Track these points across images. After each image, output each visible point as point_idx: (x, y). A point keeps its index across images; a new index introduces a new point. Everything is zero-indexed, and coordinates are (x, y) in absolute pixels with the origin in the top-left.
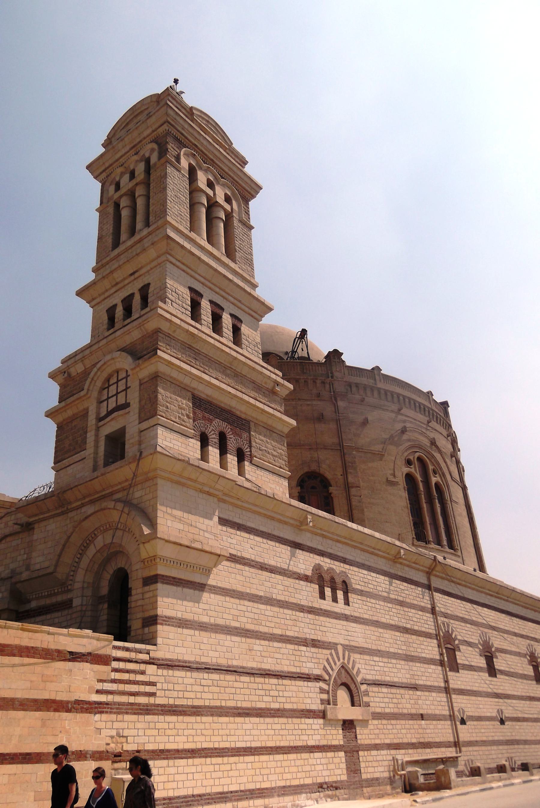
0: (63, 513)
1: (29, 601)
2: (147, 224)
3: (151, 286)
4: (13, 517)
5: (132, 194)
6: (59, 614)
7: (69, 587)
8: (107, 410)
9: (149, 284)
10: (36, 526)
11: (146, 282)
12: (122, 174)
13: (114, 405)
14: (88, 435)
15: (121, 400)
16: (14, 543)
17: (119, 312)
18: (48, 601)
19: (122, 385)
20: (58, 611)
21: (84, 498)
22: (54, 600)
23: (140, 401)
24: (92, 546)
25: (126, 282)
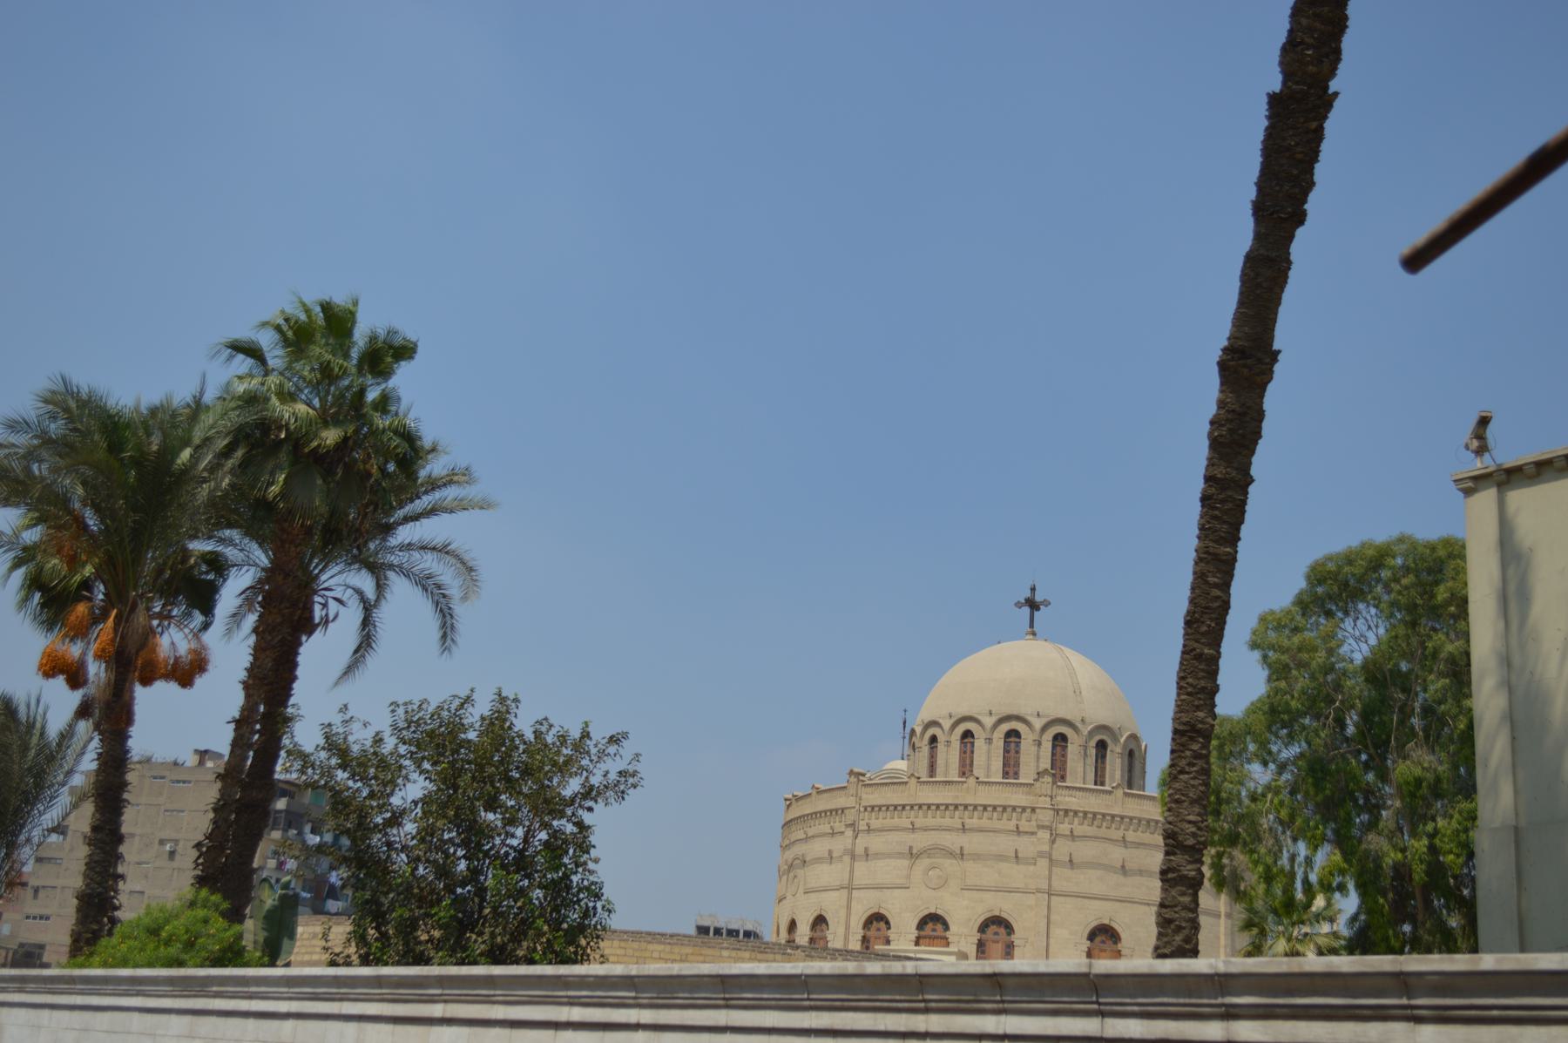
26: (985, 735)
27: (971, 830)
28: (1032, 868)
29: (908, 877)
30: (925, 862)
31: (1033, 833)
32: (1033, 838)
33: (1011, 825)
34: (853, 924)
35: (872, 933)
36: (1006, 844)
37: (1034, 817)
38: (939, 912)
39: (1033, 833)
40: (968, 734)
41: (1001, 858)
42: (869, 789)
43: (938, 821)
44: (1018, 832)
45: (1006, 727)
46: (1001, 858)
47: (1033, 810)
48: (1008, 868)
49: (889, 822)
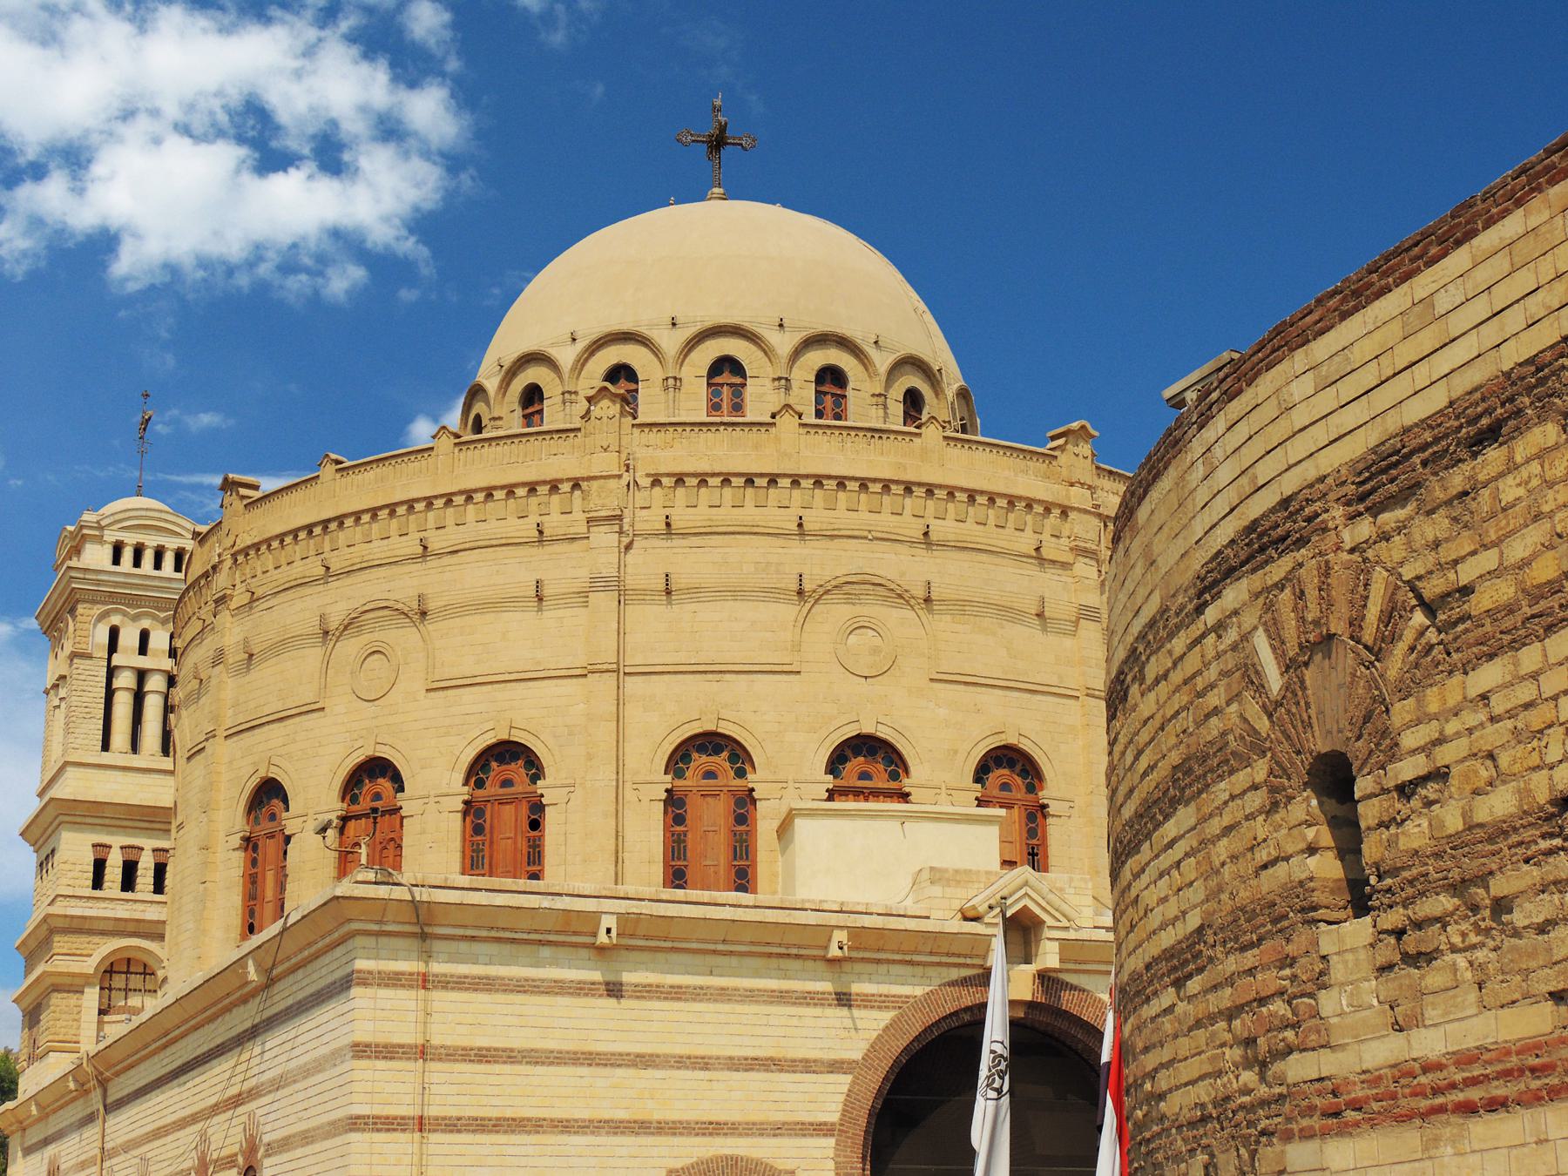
5: (142, 675)
26: (771, 371)
27: (943, 545)
28: (1068, 642)
29: (797, 647)
30: (835, 613)
31: (1065, 566)
32: (1065, 577)
33: (1026, 543)
34: (631, 762)
35: (691, 780)
36: (1020, 584)
37: (1066, 529)
38: (884, 733)
39: (1065, 566)
40: (726, 366)
41: (1008, 613)
42: (653, 437)
43: (863, 519)
44: (1038, 557)
45: (818, 358)
46: (1008, 613)
47: (1064, 513)
48: (1026, 635)
49: (726, 515)
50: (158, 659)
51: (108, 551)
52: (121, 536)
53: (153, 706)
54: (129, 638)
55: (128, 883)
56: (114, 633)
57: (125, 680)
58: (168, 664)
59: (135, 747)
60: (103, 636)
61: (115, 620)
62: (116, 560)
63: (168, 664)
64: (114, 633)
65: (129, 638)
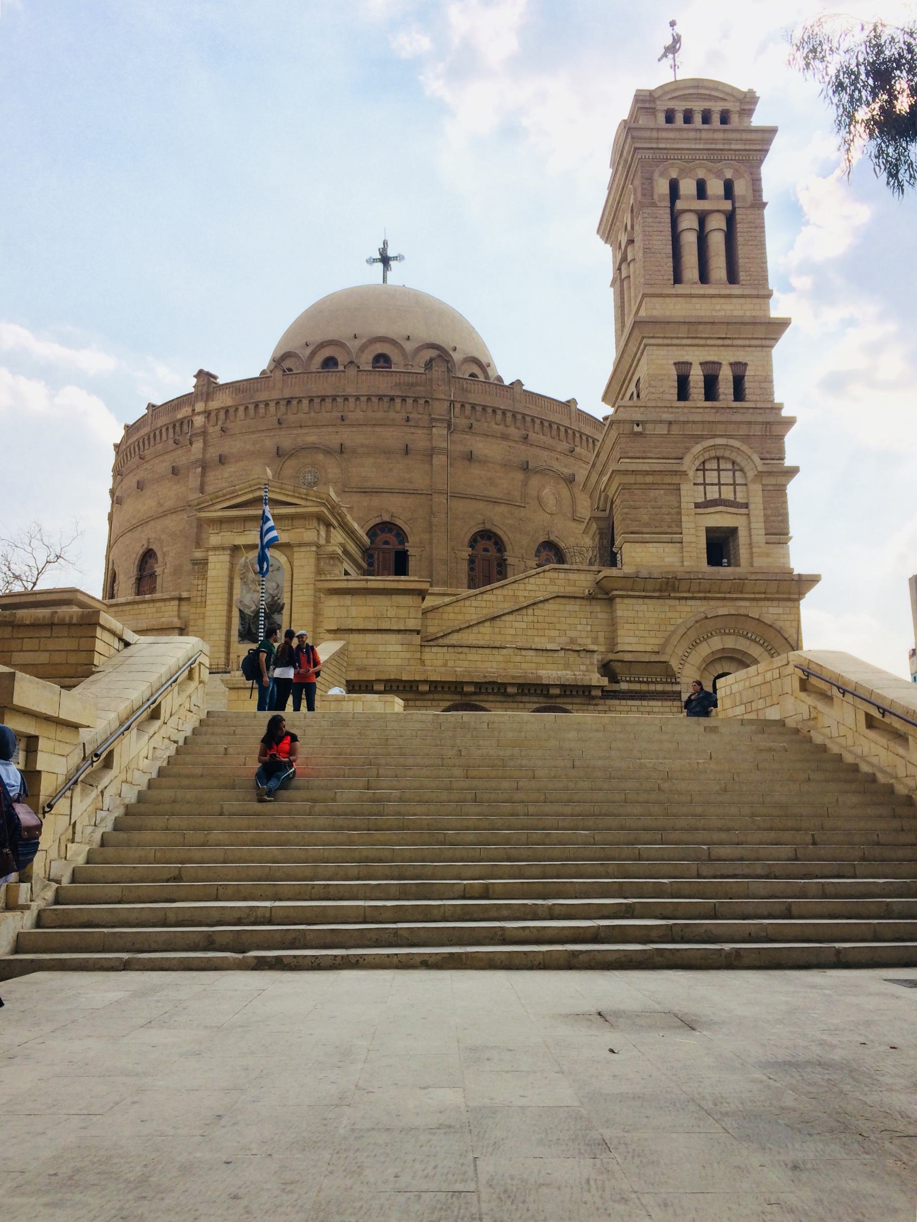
0: (658, 598)
1: (617, 682)
2: (732, 277)
3: (748, 368)
4: (562, 575)
5: (702, 217)
6: (659, 703)
7: (678, 680)
8: (705, 498)
9: (746, 364)
10: (618, 600)
11: (741, 360)
12: (683, 172)
13: (716, 496)
14: (684, 518)
15: (727, 493)
16: (569, 607)
17: (697, 376)
18: (644, 687)
19: (726, 477)
20: (658, 700)
21: (699, 592)
22: (652, 687)
23: (765, 509)
24: (704, 644)
25: (710, 342)
50: (716, 201)
51: (661, 118)
52: (671, 105)
53: (717, 241)
54: (688, 187)
55: (711, 392)
56: (674, 186)
57: (688, 222)
58: (727, 205)
59: (704, 277)
60: (662, 187)
61: (674, 175)
62: (670, 119)
63: (727, 205)
64: (674, 186)
65: (688, 187)
